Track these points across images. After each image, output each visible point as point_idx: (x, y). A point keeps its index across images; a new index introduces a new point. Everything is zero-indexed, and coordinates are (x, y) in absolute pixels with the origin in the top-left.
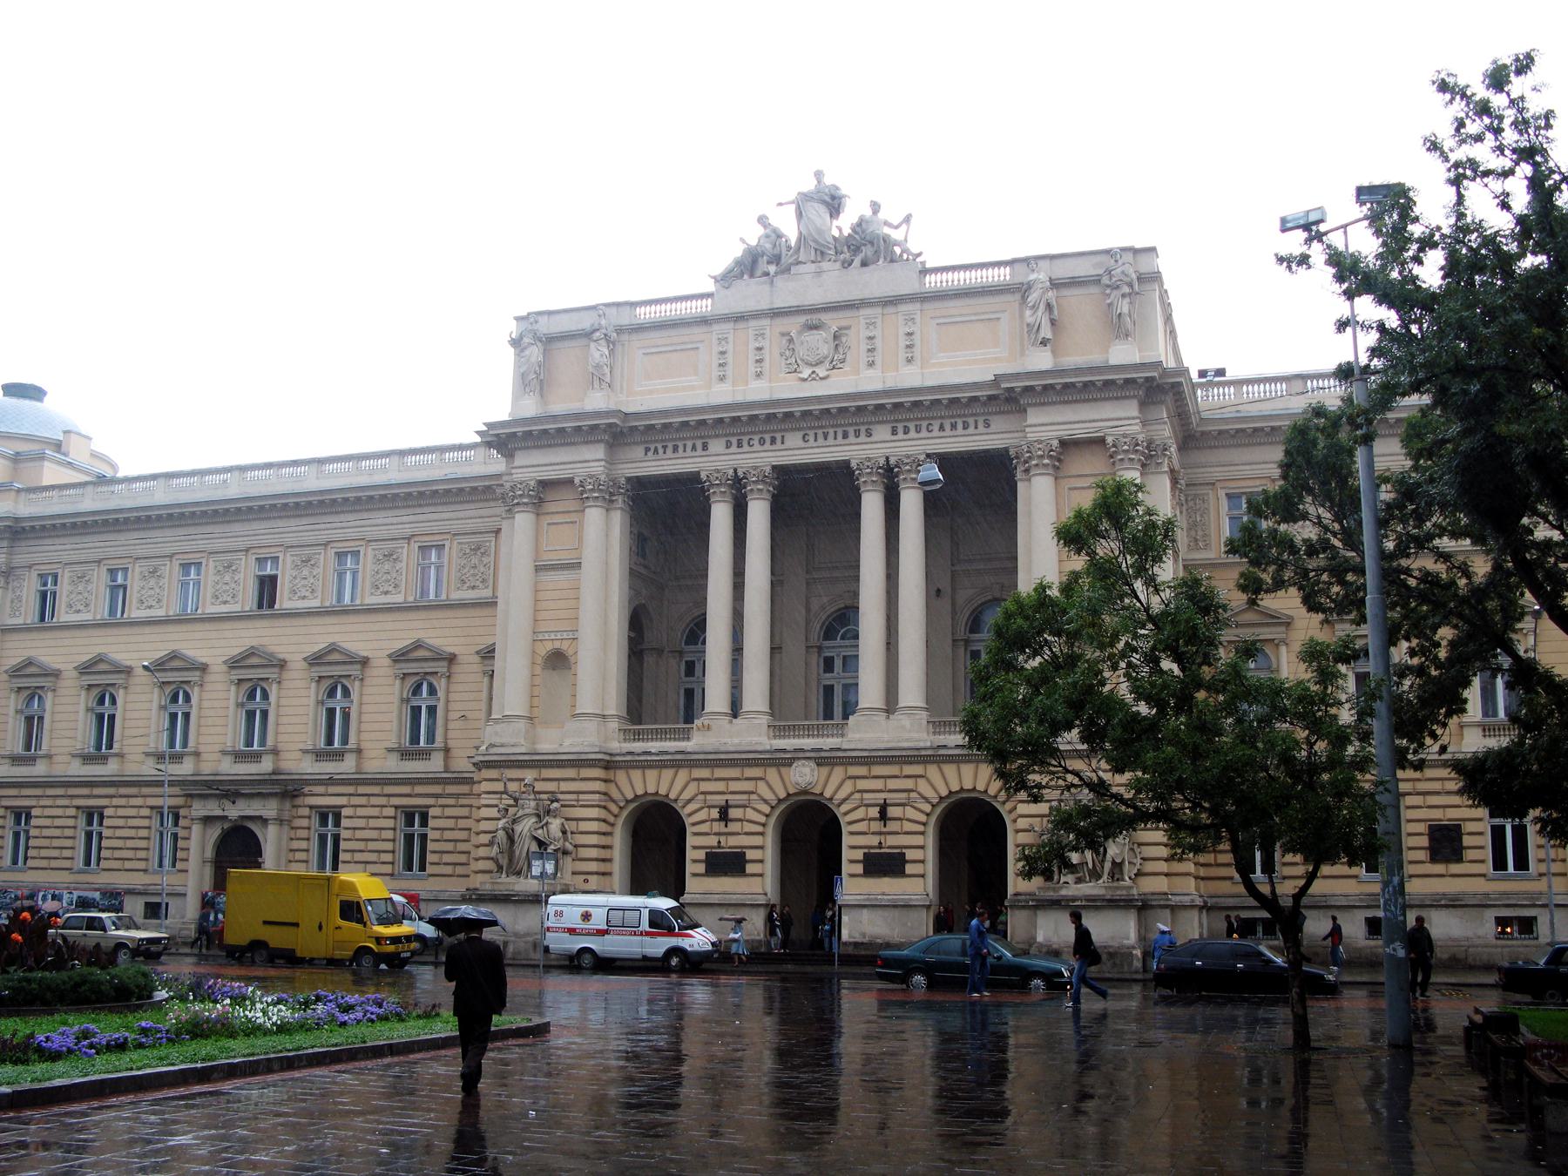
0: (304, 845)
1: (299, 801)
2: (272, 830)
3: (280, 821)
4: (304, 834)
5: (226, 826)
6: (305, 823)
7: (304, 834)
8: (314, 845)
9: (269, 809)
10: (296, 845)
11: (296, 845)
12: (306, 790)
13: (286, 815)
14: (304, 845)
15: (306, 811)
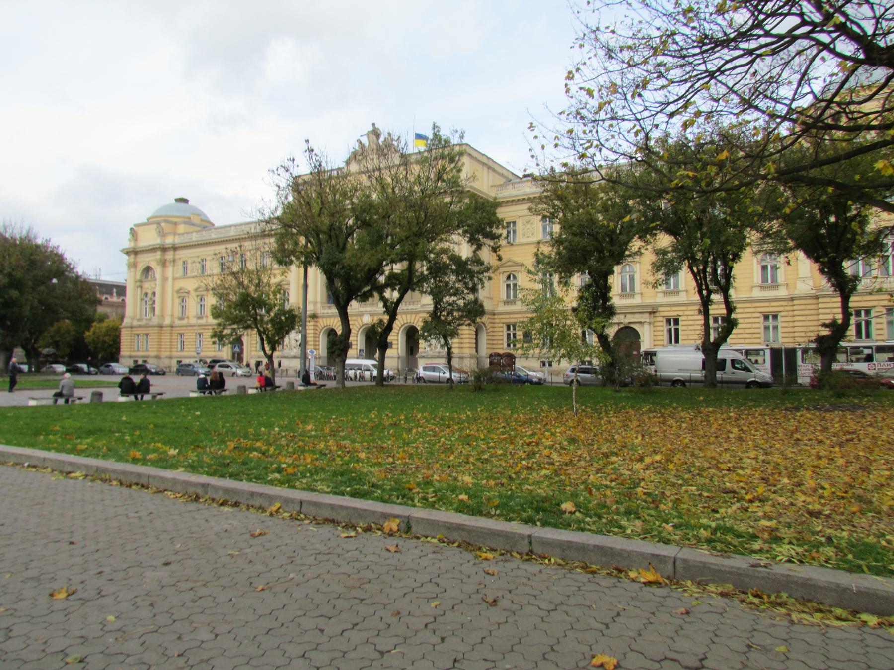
0: (660, 333)
1: (657, 314)
2: (646, 326)
3: (650, 323)
4: (661, 328)
5: (622, 326)
6: (661, 324)
7: (661, 328)
8: (665, 334)
9: (645, 318)
10: (656, 333)
11: (656, 333)
12: (660, 309)
13: (652, 320)
14: (660, 333)
15: (661, 319)
